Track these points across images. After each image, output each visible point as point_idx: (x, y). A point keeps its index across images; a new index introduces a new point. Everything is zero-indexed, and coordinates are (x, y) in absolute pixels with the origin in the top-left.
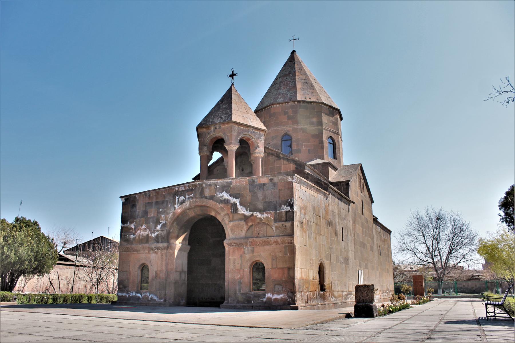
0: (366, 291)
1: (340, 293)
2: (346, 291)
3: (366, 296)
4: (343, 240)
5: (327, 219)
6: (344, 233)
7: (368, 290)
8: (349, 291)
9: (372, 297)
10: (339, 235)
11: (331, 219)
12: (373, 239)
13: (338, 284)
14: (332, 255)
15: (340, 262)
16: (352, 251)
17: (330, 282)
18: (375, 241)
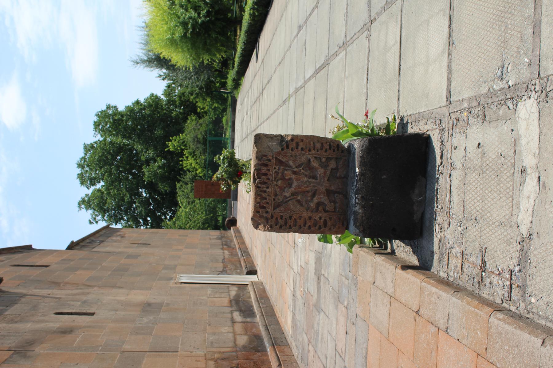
0: (288, 174)
1: (238, 328)
2: (232, 312)
3: (314, 177)
4: (93, 314)
5: (6, 358)
6: (73, 309)
7: (280, 163)
8: (231, 306)
9: (318, 145)
10: (74, 324)
11: (14, 344)
12: (113, 253)
13: (214, 334)
14: (126, 347)
15: (150, 325)
16: (128, 295)
17: (209, 356)
18: (120, 250)
